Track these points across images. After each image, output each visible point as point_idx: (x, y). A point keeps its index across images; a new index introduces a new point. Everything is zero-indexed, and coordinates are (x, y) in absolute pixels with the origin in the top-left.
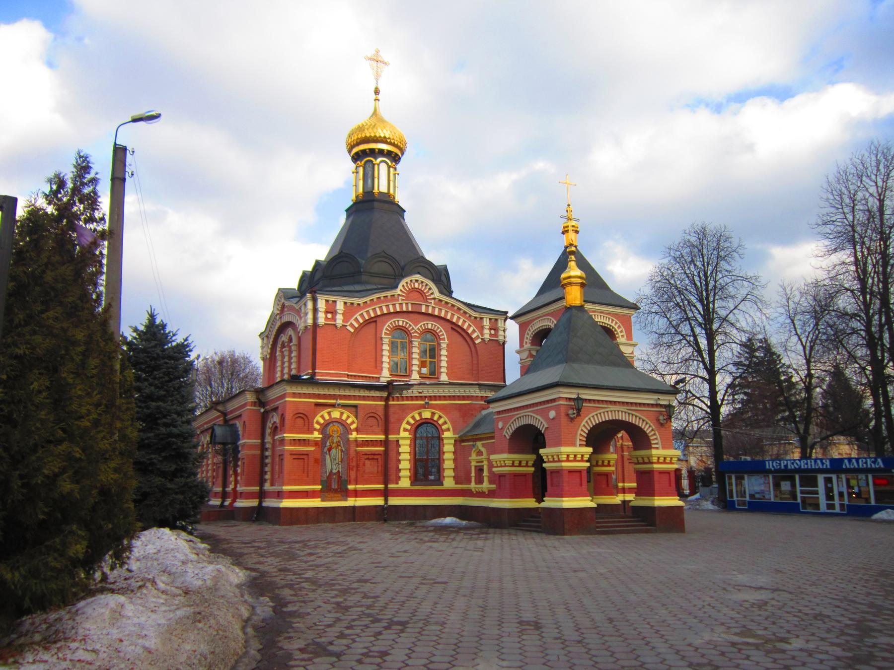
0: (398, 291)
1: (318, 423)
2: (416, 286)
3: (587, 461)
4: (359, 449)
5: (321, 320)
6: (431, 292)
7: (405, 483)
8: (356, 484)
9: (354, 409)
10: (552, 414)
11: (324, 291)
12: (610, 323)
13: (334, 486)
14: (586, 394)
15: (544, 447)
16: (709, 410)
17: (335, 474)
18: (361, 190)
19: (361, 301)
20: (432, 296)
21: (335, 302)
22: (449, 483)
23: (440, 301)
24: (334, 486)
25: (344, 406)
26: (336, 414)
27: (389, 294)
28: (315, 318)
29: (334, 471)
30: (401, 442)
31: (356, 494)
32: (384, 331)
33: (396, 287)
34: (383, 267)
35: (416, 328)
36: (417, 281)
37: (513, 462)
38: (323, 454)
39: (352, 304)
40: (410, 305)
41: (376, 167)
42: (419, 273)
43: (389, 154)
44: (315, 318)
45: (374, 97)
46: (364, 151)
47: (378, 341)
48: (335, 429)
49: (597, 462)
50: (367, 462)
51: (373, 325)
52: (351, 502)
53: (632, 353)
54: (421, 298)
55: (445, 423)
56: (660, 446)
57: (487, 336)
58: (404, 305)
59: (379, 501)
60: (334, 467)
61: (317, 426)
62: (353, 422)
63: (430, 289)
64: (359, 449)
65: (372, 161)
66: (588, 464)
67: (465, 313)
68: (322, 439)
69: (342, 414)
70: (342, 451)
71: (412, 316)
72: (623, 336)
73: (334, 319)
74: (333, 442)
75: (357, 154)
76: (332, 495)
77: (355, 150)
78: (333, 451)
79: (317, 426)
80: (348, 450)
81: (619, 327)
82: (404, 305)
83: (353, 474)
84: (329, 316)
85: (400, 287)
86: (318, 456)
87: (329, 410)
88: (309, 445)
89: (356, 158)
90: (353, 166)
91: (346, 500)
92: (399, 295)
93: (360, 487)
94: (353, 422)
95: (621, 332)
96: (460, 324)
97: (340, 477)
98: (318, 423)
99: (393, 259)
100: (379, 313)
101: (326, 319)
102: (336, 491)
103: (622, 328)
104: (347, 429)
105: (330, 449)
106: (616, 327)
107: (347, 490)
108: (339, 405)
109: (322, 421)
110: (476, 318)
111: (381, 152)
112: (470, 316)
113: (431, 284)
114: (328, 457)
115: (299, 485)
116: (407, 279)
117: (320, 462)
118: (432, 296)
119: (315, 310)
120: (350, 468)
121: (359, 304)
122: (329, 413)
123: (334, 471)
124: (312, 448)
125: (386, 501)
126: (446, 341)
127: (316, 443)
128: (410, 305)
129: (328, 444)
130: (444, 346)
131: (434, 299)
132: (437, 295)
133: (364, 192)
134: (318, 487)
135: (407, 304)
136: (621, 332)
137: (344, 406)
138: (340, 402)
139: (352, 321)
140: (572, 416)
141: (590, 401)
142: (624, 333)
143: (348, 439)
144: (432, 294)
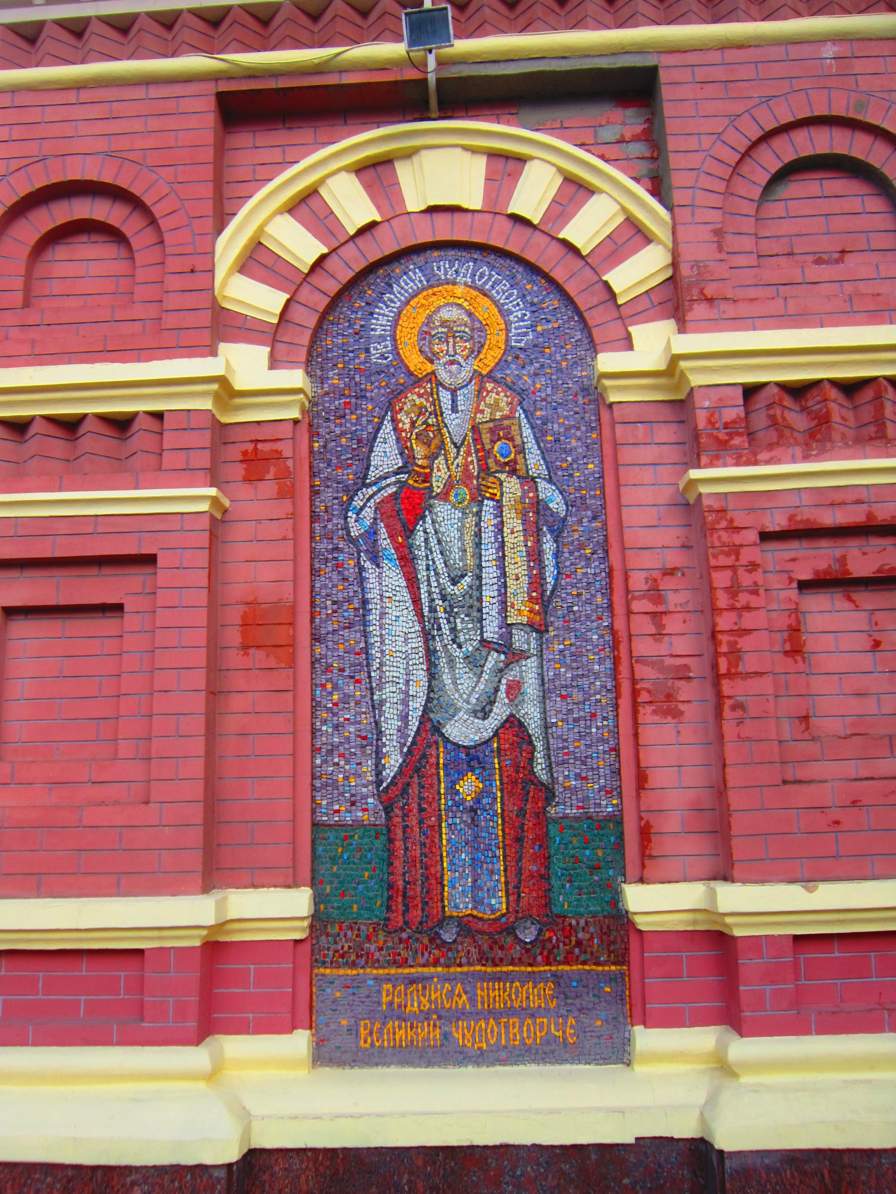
1: (258, 261)
4: (716, 478)
9: (620, 122)
13: (473, 887)
17: (472, 757)
24: (473, 887)
26: (444, 170)
29: (464, 730)
31: (725, 980)
38: (328, 554)
48: (440, 322)
50: (825, 614)
52: (665, 1084)
60: (463, 686)
61: (263, 300)
62: (631, 235)
64: (716, 478)
68: (311, 422)
69: (506, 166)
70: (536, 515)
74: (434, 438)
76: (442, 990)
78: (446, 520)
80: (600, 501)
83: (674, 753)
86: (264, 569)
87: (368, 140)
88: (158, 472)
93: (756, 904)
94: (631, 235)
97: (528, 794)
98: (258, 261)
102: (490, 943)
105: (408, 508)
107: (618, 925)
109: (301, 246)
114: (386, 581)
117: (288, 637)
120: (632, 696)
122: (376, 172)
124: (194, 498)
127: (237, 451)
129: (385, 456)
134: (277, 909)
143: (593, 394)
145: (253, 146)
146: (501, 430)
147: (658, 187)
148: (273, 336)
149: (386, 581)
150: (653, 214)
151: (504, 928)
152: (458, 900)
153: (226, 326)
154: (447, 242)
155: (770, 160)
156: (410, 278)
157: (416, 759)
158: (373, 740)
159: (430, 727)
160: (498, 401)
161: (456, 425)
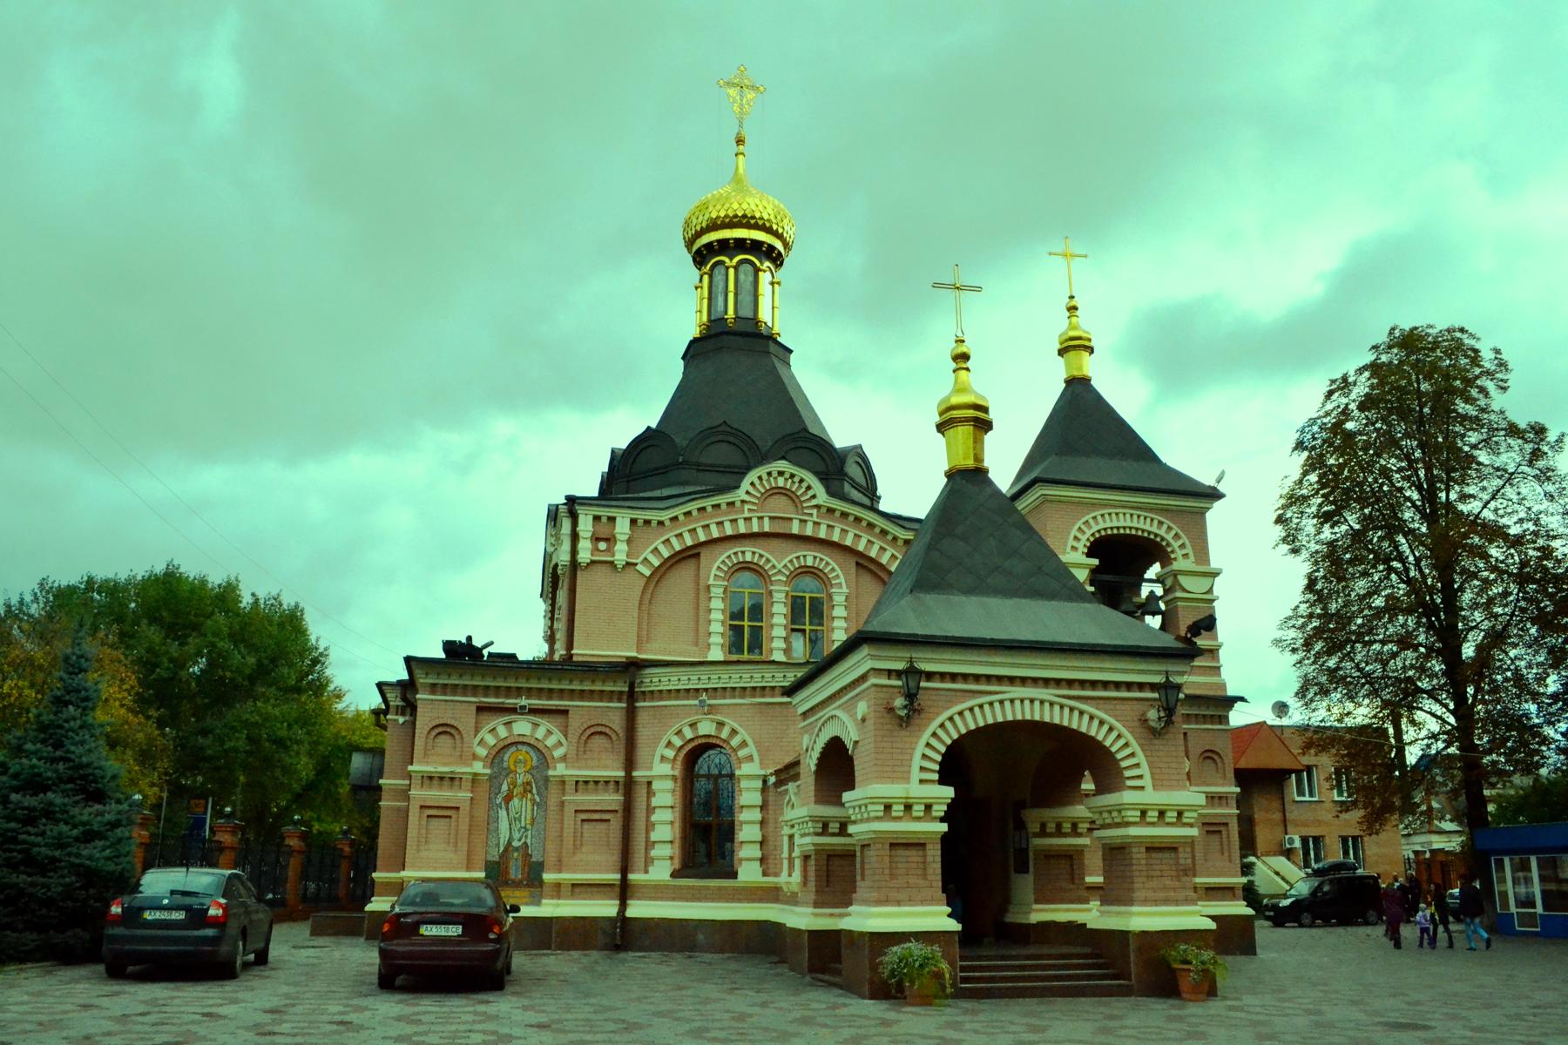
0: (741, 494)
2: (781, 482)
3: (942, 820)
5: (584, 555)
6: (810, 493)
7: (661, 872)
8: (560, 871)
10: (862, 708)
12: (1154, 529)
14: (930, 662)
15: (852, 787)
16: (1452, 720)
17: (517, 849)
18: (705, 319)
19: (665, 516)
20: (814, 502)
21: (612, 519)
22: (749, 873)
23: (831, 511)
25: (534, 711)
26: (522, 727)
27: (728, 497)
28: (574, 552)
29: (516, 844)
30: (655, 786)
31: (558, 890)
32: (714, 571)
34: (721, 454)
35: (779, 566)
36: (781, 473)
37: (825, 826)
39: (647, 522)
40: (766, 520)
41: (732, 271)
42: (783, 458)
44: (574, 552)
45: (735, 148)
46: (709, 246)
47: (701, 592)
49: (1043, 826)
51: (691, 563)
53: (1210, 591)
54: (792, 508)
55: (744, 744)
56: (1147, 781)
58: (755, 521)
59: (606, 908)
60: (516, 835)
63: (809, 488)
65: (722, 263)
66: (944, 827)
67: (884, 532)
71: (775, 543)
72: (1185, 556)
73: (610, 550)
75: (699, 251)
77: (695, 248)
78: (516, 801)
79: (482, 752)
81: (1177, 536)
82: (755, 521)
84: (602, 546)
85: (745, 485)
87: (507, 718)
89: (700, 258)
90: (696, 273)
91: (538, 903)
95: (1182, 546)
96: (873, 554)
97: (527, 856)
99: (738, 433)
100: (702, 538)
101: (596, 550)
103: (1184, 539)
104: (544, 759)
106: (1169, 537)
108: (523, 707)
111: (741, 245)
112: (895, 539)
113: (811, 479)
114: (503, 813)
115: (450, 870)
116: (761, 471)
118: (814, 502)
119: (575, 537)
121: (661, 523)
123: (516, 844)
125: (623, 906)
126: (845, 590)
128: (766, 520)
129: (505, 787)
130: (839, 599)
131: (818, 507)
132: (822, 497)
133: (709, 320)
135: (761, 518)
136: (1182, 546)
137: (534, 711)
138: (523, 702)
139: (647, 554)
140: (903, 713)
141: (943, 676)
142: (1189, 550)
144: (814, 497)
145: (484, 717)
146: (529, 783)
147: (566, 736)
148: (483, 760)
149: (503, 813)
150: (563, 740)
151: (521, 882)
152: (512, 876)
153: (475, 757)
154: (518, 743)
155: (589, 732)
156: (513, 749)
157: (506, 850)
158: (498, 845)
159: (509, 843)
160: (529, 777)
161: (519, 781)
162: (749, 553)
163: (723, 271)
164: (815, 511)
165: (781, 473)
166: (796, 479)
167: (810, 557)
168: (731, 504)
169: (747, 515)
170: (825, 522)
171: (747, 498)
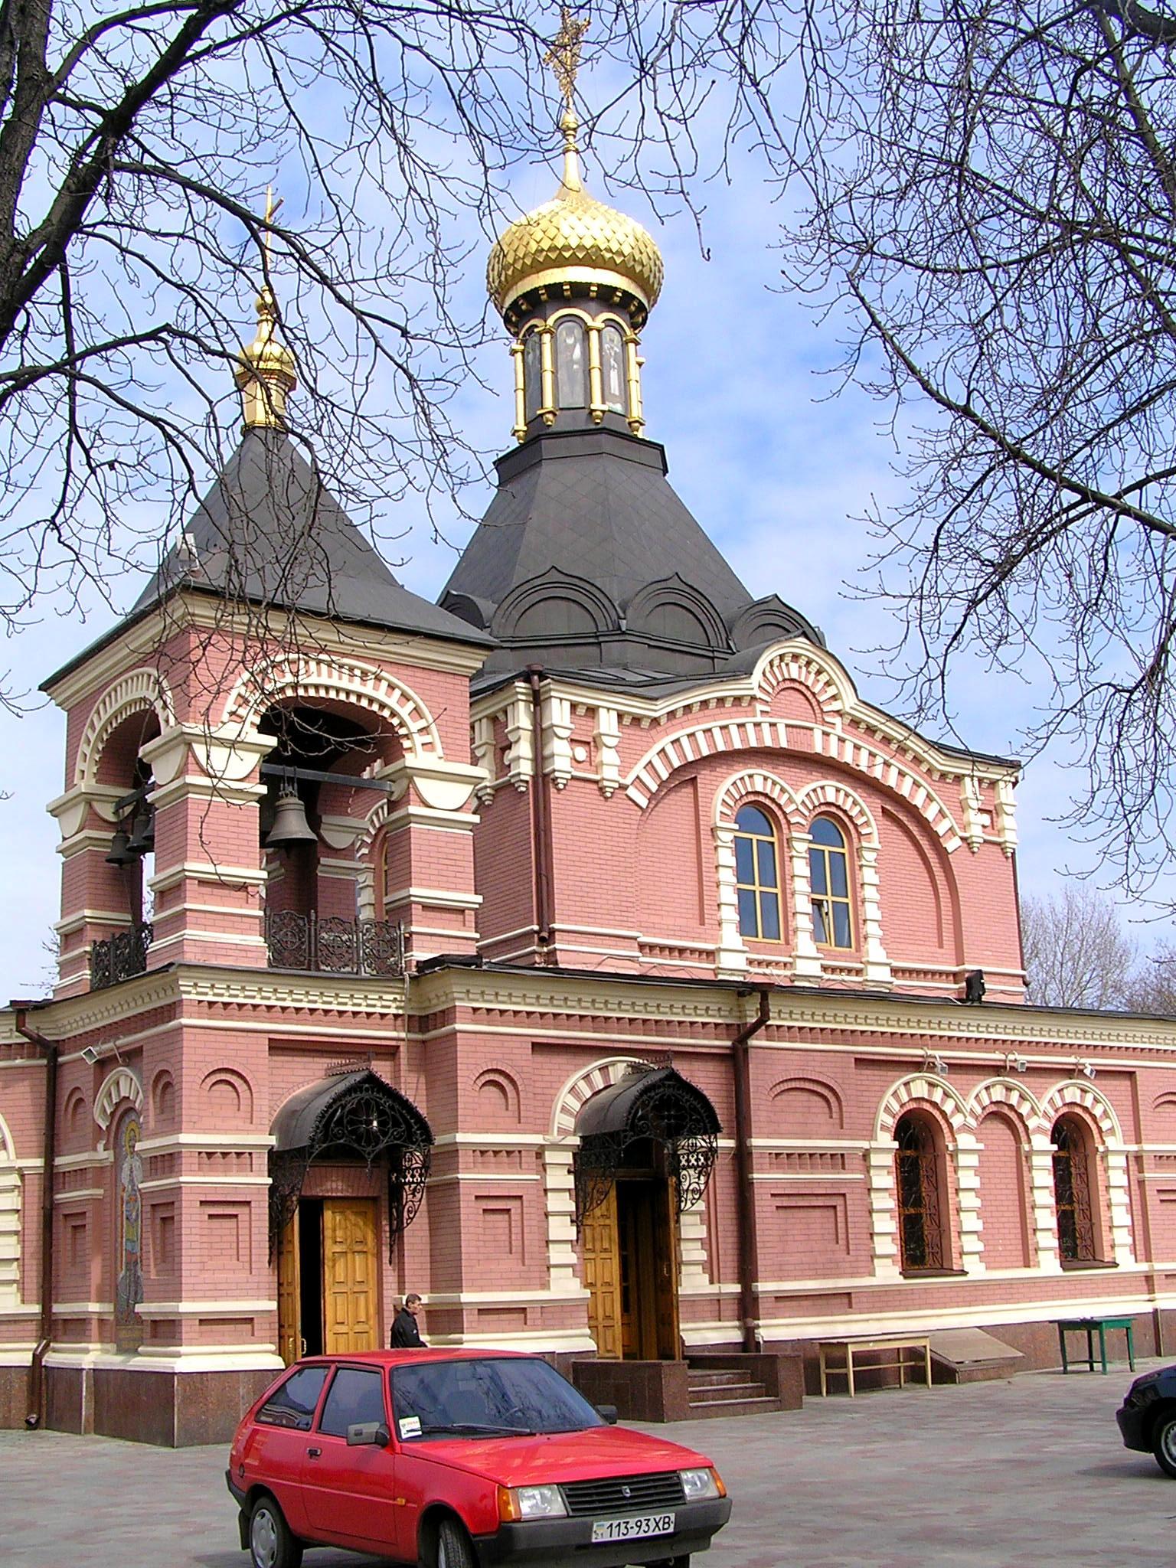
2: (794, 671)
11: (569, 678)
21: (592, 711)
28: (540, 758)
33: (749, 673)
36: (796, 657)
41: (594, 335)
43: (606, 296)
44: (540, 758)
46: (554, 290)
47: (701, 833)
57: (976, 832)
92: (753, 698)
110: (943, 776)
118: (836, 706)
121: (655, 721)
128: (781, 728)
139: (638, 770)
144: (834, 698)
162: (760, 778)
163: (578, 332)
164: (837, 720)
165: (796, 657)
166: (814, 668)
167: (832, 790)
168: (738, 700)
169: (758, 719)
170: (851, 740)
171: (760, 695)
